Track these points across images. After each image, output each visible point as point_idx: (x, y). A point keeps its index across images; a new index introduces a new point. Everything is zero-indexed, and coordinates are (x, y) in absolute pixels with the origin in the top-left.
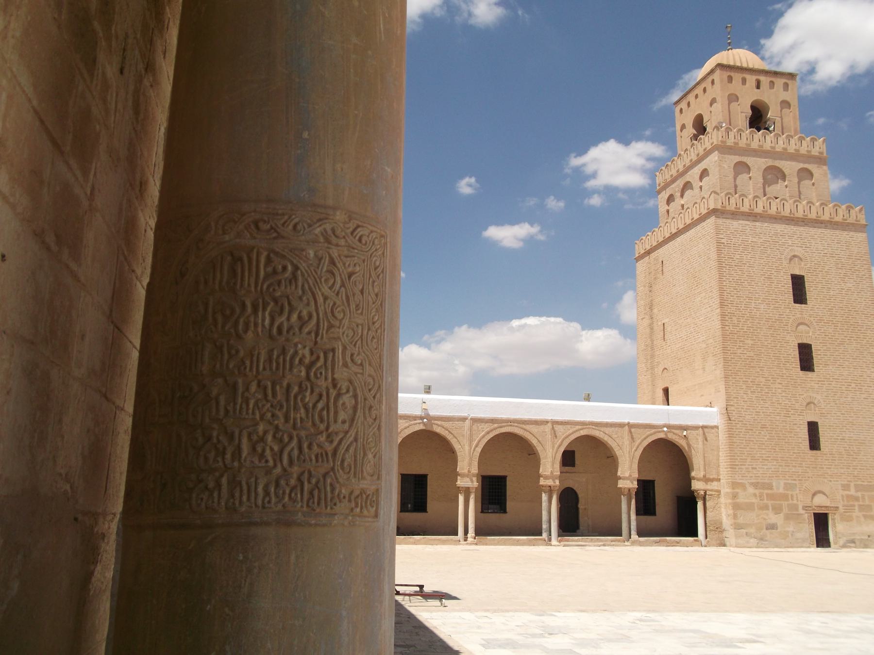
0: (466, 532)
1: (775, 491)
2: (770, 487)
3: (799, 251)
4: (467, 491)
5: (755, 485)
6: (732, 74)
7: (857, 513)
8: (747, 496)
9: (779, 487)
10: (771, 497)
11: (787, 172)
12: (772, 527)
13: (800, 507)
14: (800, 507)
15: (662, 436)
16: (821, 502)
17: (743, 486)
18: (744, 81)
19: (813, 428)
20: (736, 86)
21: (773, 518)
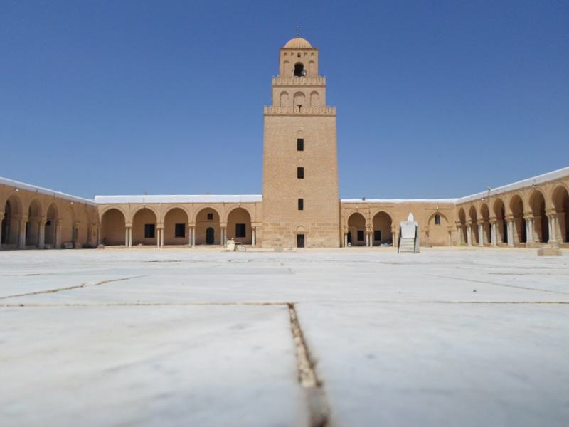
0: (160, 244)
1: (281, 226)
2: (279, 225)
3: (302, 129)
4: (160, 229)
5: (271, 224)
6: (286, 51)
7: (317, 234)
8: (269, 228)
9: (283, 224)
10: (279, 229)
11: (305, 93)
12: (278, 240)
13: (291, 232)
14: (291, 232)
15: (238, 207)
16: (301, 230)
17: (267, 225)
18: (292, 54)
19: (301, 202)
20: (288, 57)
21: (279, 237)
